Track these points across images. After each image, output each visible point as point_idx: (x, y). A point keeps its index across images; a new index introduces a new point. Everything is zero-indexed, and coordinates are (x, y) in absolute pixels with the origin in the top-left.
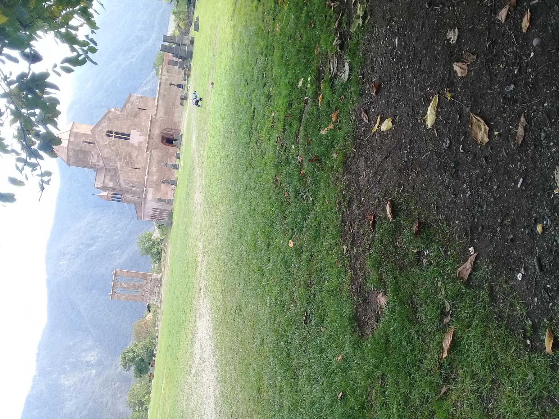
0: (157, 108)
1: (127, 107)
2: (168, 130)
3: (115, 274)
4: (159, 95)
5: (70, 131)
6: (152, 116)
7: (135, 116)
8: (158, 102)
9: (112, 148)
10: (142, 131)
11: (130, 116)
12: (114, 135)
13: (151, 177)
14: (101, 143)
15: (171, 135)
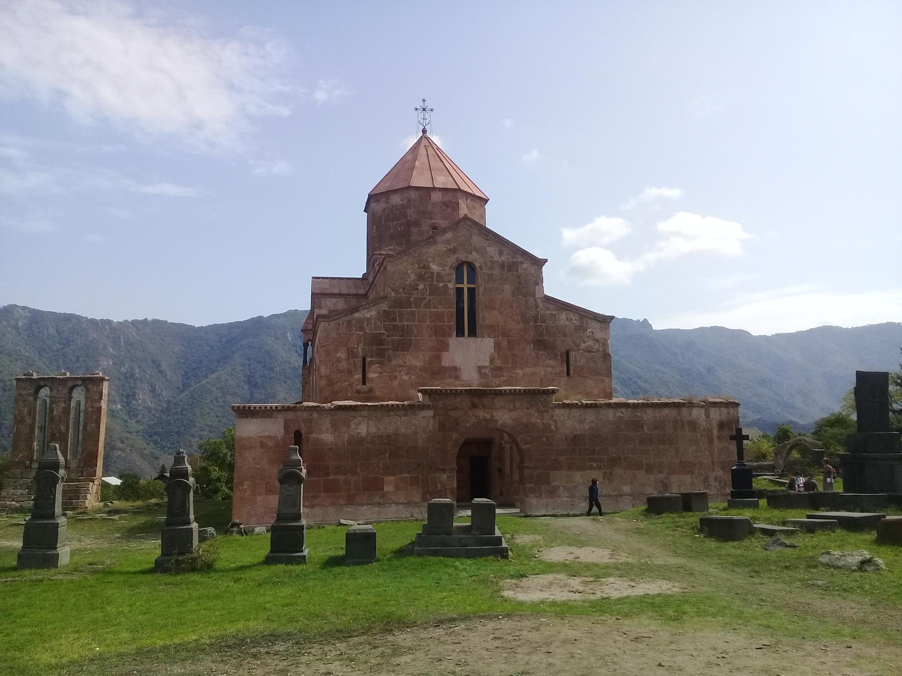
0: (587, 406)
1: (563, 316)
2: (517, 458)
3: (91, 380)
4: (635, 406)
5: (459, 190)
6: (553, 390)
7: (541, 344)
8: (609, 405)
9: (421, 287)
10: (497, 371)
11: (536, 327)
12: (465, 286)
13: (326, 422)
14: (431, 250)
15: (500, 471)
